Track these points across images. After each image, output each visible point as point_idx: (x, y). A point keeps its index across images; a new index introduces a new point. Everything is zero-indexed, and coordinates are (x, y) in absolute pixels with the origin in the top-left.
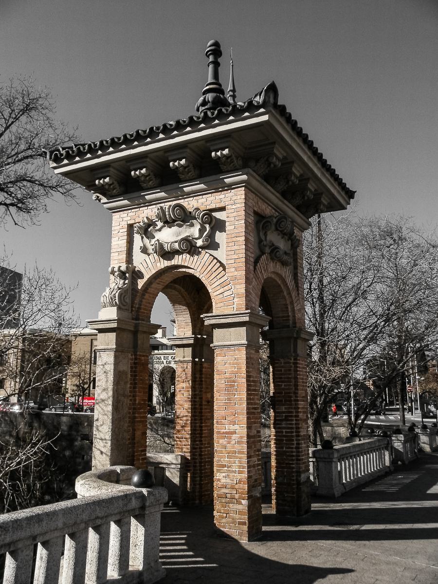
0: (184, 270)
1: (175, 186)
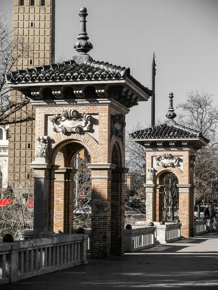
0: (77, 141)
1: (72, 100)
